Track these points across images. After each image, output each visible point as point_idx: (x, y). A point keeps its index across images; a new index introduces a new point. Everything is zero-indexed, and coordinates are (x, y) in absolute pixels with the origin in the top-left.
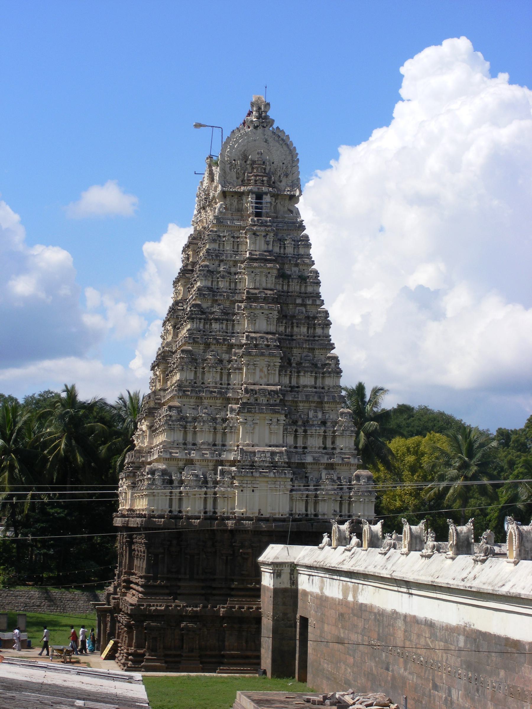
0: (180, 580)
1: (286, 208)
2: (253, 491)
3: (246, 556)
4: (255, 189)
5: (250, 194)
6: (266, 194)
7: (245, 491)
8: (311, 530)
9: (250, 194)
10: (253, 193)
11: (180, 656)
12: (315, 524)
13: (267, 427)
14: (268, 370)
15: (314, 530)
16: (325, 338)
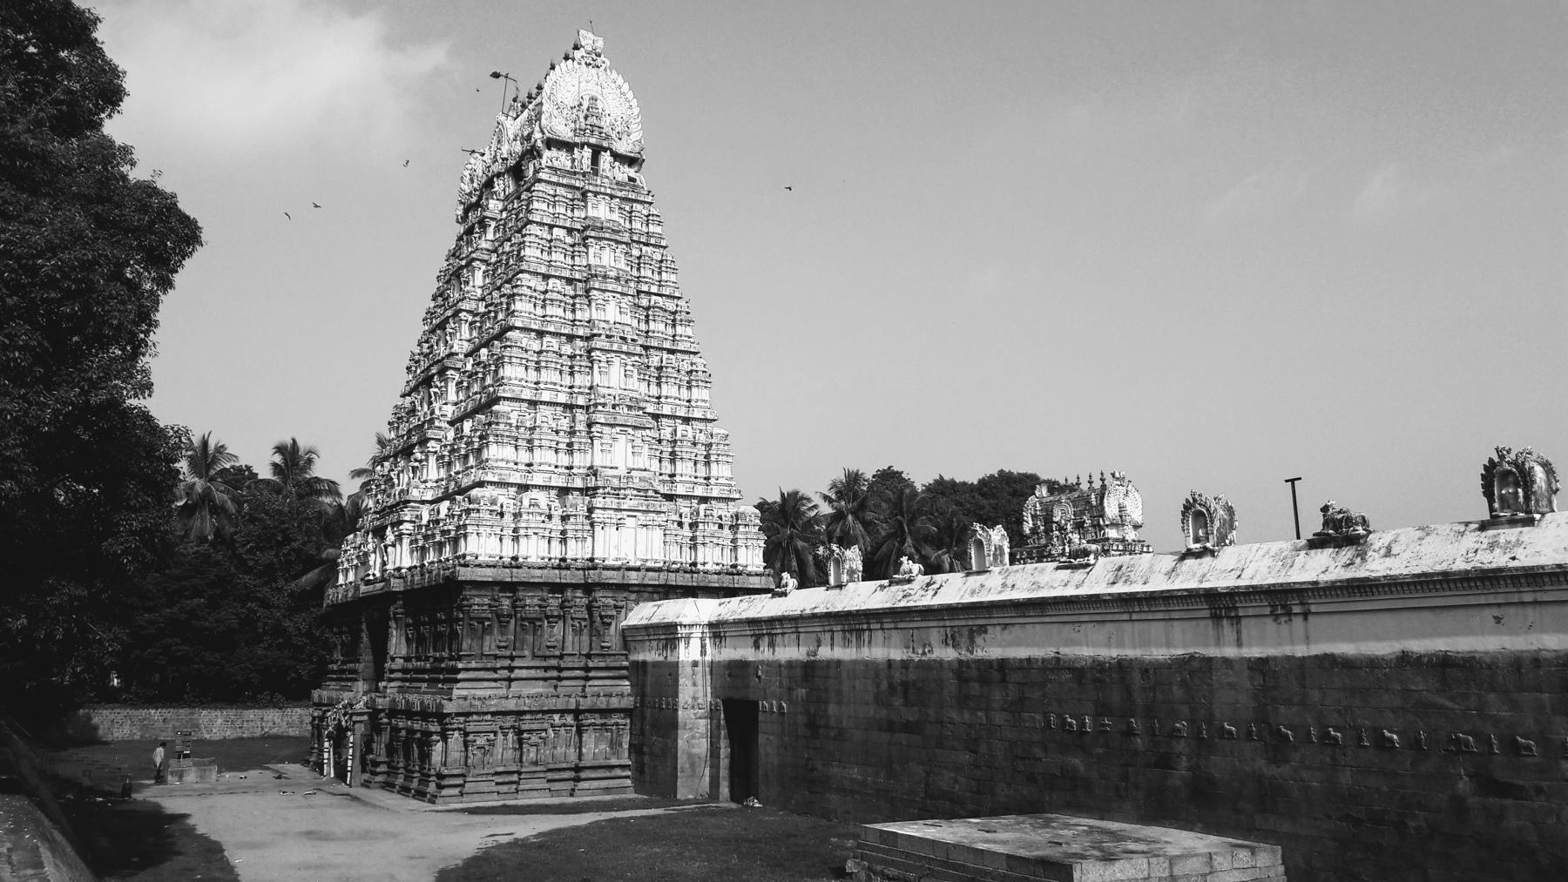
0: (512, 658)
1: (626, 175)
2: (617, 529)
3: (609, 621)
4: (593, 141)
5: (586, 146)
6: (605, 150)
7: (607, 529)
8: (690, 584)
9: (586, 146)
10: (589, 145)
11: (519, 773)
12: (695, 575)
13: (630, 445)
14: (625, 371)
15: (695, 584)
16: (686, 339)
